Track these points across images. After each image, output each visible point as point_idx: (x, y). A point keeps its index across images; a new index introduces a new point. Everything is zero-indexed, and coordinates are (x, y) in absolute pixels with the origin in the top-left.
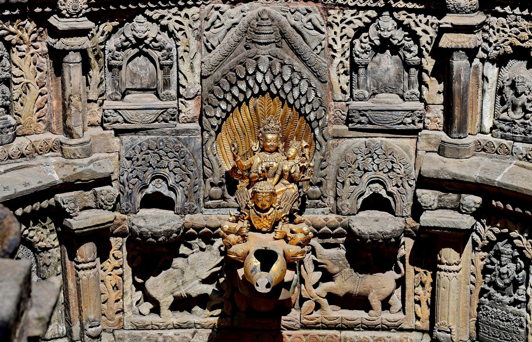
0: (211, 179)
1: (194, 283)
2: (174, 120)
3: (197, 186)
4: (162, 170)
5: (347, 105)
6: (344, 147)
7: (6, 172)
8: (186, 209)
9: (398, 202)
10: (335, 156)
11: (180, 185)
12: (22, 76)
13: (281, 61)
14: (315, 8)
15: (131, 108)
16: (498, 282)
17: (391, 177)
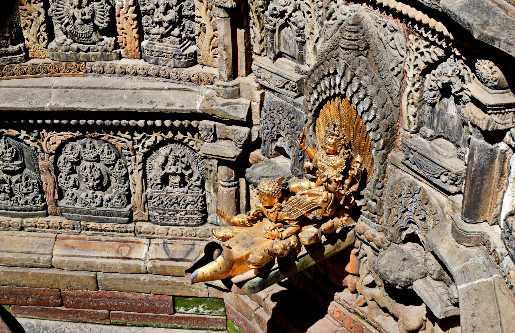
2: (295, 92)
3: (301, 157)
5: (411, 137)
6: (398, 176)
7: (169, 89)
10: (390, 181)
12: (200, 17)
13: (353, 70)
14: (401, 28)
15: (268, 69)
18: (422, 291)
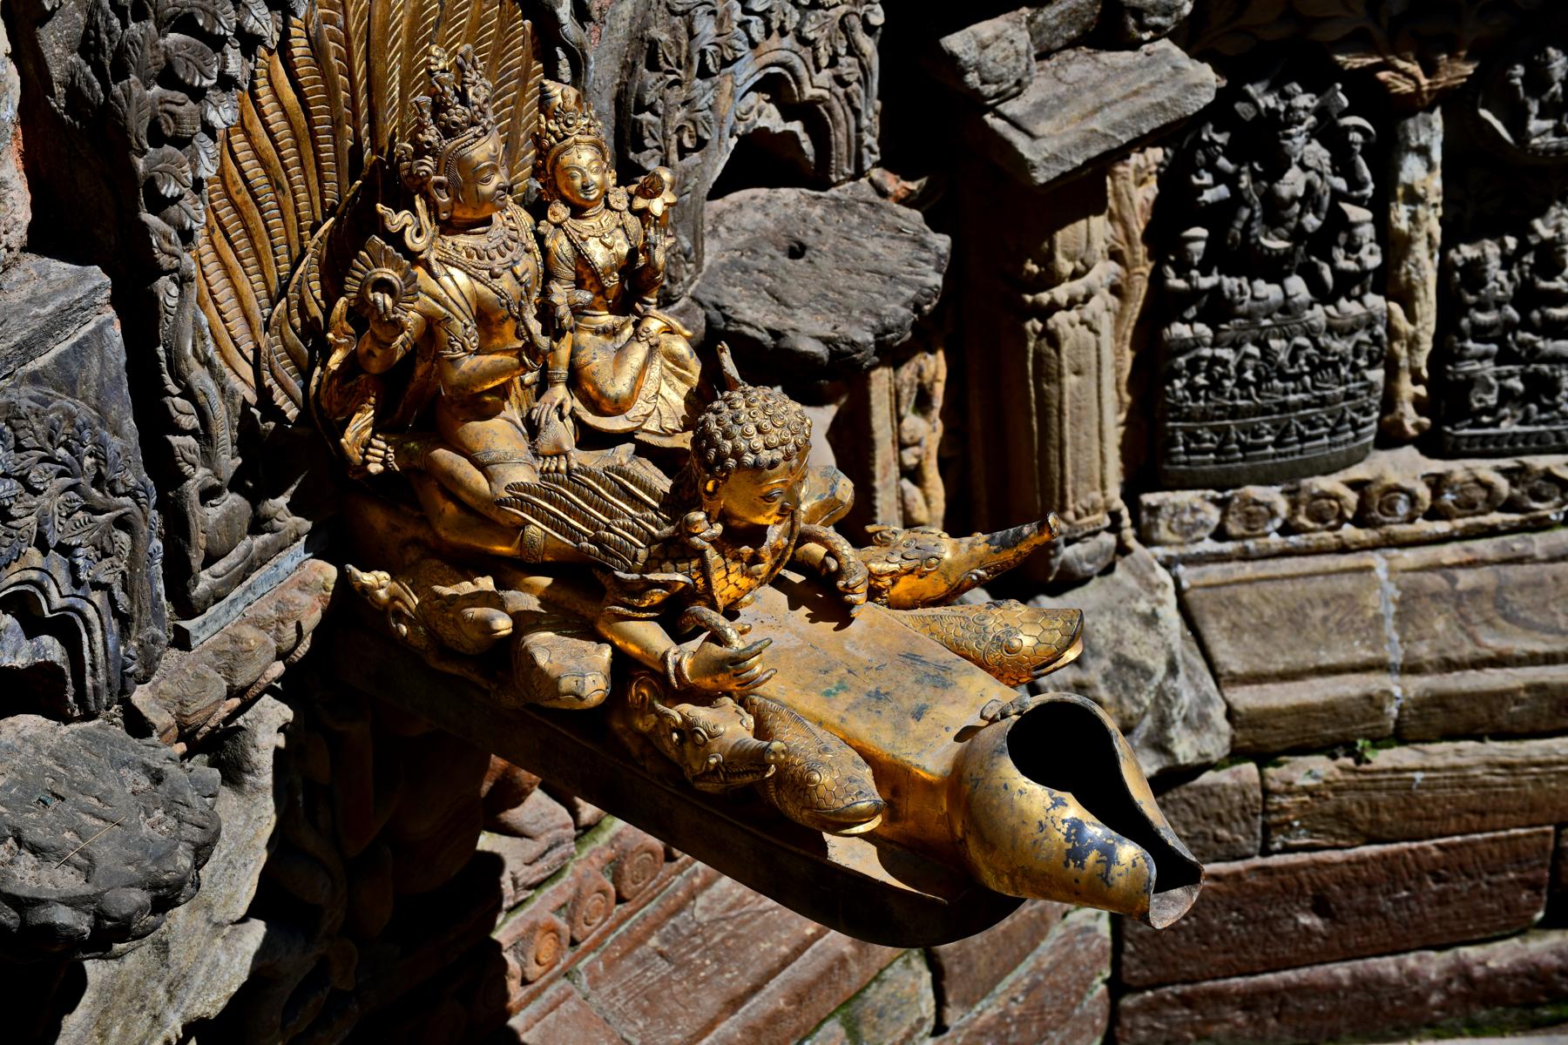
0: (199, 476)
1: (208, 960)
4: (15, 567)
8: (130, 675)
9: (837, 124)
11: (96, 586)
16: (1263, 240)
17: (811, 36)
18: (1097, 124)
